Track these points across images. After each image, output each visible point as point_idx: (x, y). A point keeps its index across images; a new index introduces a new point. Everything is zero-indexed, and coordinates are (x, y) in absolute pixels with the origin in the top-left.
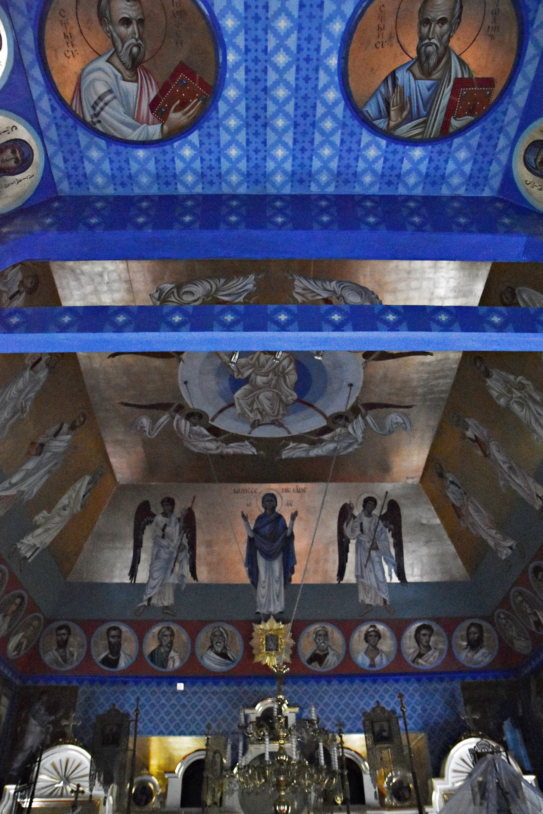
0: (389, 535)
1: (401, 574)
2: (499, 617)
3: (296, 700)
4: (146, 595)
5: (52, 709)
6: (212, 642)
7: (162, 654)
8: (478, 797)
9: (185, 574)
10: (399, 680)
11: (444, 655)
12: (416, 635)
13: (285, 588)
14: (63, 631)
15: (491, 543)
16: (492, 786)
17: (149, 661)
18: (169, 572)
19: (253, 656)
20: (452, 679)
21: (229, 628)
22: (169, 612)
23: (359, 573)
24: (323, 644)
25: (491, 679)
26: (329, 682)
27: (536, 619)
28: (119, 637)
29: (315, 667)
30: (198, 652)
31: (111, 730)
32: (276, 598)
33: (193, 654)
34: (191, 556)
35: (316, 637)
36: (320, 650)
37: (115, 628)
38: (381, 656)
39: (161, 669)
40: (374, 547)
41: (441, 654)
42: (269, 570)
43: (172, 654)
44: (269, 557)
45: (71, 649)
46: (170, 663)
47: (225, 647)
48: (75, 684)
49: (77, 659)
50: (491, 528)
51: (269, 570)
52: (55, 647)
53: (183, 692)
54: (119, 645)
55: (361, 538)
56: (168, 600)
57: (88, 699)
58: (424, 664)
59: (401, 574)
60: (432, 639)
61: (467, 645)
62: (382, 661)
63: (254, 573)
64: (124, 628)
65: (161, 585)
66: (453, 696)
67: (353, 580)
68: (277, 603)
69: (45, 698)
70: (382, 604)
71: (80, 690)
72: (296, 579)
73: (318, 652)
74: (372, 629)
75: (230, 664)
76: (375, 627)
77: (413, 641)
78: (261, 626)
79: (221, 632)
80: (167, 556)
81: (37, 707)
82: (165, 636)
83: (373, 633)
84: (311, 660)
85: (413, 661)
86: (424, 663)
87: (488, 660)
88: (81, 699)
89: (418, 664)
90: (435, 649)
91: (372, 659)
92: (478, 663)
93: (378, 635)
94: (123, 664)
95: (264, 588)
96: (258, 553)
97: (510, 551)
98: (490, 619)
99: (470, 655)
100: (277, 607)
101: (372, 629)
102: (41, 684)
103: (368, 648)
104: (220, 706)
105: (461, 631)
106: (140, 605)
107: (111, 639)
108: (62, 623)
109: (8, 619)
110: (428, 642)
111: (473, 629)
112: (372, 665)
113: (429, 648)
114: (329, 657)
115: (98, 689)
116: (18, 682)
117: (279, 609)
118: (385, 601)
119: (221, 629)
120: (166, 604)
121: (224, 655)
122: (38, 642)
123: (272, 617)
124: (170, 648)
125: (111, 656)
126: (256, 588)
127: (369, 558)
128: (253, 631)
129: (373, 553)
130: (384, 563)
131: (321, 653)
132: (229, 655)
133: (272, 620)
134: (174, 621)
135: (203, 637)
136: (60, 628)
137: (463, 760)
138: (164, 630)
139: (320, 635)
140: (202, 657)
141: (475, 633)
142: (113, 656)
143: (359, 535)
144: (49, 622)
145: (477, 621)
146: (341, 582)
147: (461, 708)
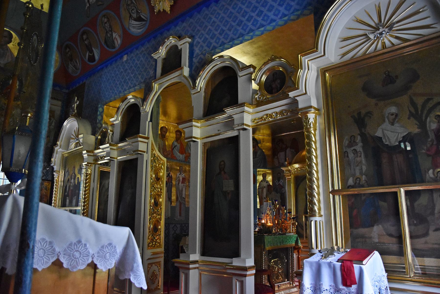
46: (115, 41)
94: (97, 57)
121: (139, 19)
132: (142, 16)
142: (91, 54)
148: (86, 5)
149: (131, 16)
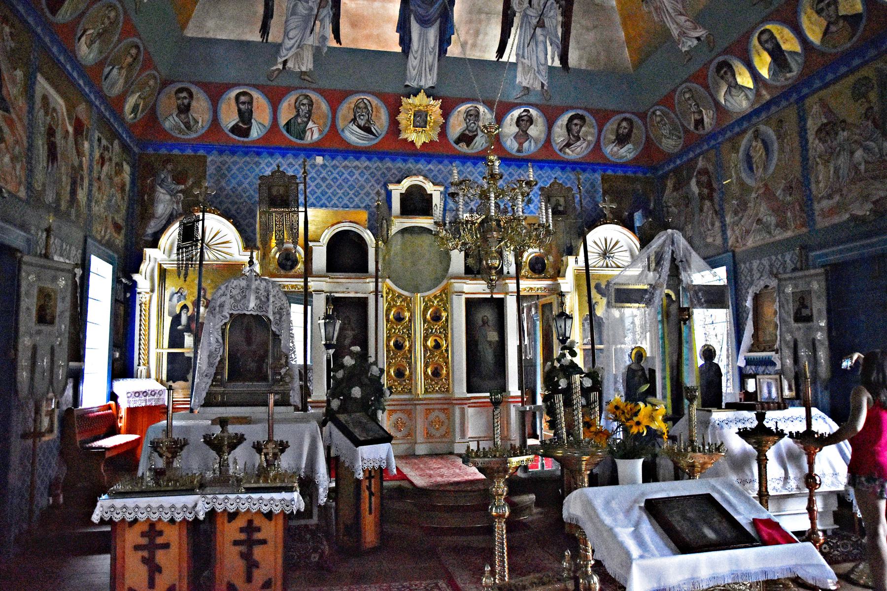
0: (559, 11)
1: (564, 58)
2: (654, 113)
3: (440, 179)
4: (281, 57)
5: (179, 179)
6: (355, 116)
7: (299, 124)
8: (653, 265)
9: (327, 35)
10: (544, 166)
11: (592, 146)
12: (567, 125)
13: (439, 60)
14: (184, 94)
15: (675, 33)
16: (667, 257)
17: (285, 133)
18: (308, 32)
19: (399, 131)
20: (594, 171)
21: (375, 101)
22: (307, 78)
23: (521, 53)
24: (473, 125)
25: (629, 174)
26: (475, 164)
27: (697, 117)
28: (250, 103)
29: (463, 148)
30: (340, 124)
31: (278, 191)
32: (428, 70)
33: (334, 125)
34: (334, 14)
35: (467, 116)
36: (470, 131)
37: (244, 94)
38: (530, 142)
39: (299, 141)
40: (541, 24)
41: (589, 145)
42: (423, 37)
43: (310, 125)
44: (425, 23)
45: (195, 115)
46: (308, 134)
47: (368, 120)
48: (201, 152)
49: (203, 127)
50: (681, 14)
51: (423, 37)
52: (175, 112)
53: (324, 166)
54: (251, 112)
55: (528, 12)
56: (307, 65)
57: (219, 169)
58: (571, 154)
59: (564, 58)
60: (583, 129)
61: (615, 140)
62: (530, 148)
63: (405, 41)
64: (256, 94)
65: (298, 47)
66: (593, 185)
67: (513, 59)
68: (429, 77)
69: (169, 167)
70: (539, 88)
71: (209, 159)
72: (453, 51)
73: (467, 132)
74: (525, 114)
75: (372, 139)
76: (528, 111)
77: (564, 131)
78: (410, 101)
79: (365, 104)
80: (306, 12)
81: (163, 176)
82: (303, 105)
83: (525, 118)
84: (458, 141)
85: (561, 150)
86: (570, 153)
87: (630, 156)
88: (211, 170)
89: (565, 153)
90: (584, 140)
91: (521, 144)
92: (622, 157)
93: (531, 121)
95: (415, 58)
96: (412, 18)
97: (696, 42)
98: (643, 116)
99: (615, 149)
100: (429, 80)
101: (525, 114)
102: (164, 151)
103: (518, 133)
104: (362, 180)
105: (611, 126)
106: (275, 68)
107: (242, 107)
108: (180, 85)
109: (124, 72)
110: (579, 132)
111: (624, 124)
112: (519, 151)
113: (578, 138)
114: (477, 138)
115: (228, 159)
116: (136, 150)
117: (430, 84)
118: (543, 85)
119: (365, 101)
120: (304, 69)
121: (367, 130)
122: (155, 105)
123: (422, 91)
124: (309, 119)
125: (240, 124)
126: (408, 57)
127: (533, 36)
128: (402, 105)
129: (539, 31)
130: (548, 43)
131: (470, 135)
132: (373, 129)
133: (422, 95)
134: (314, 90)
135: (345, 109)
136: (181, 90)
137: (606, 240)
138: (301, 98)
139: (471, 115)
140: (343, 130)
141: (625, 128)
142: (245, 124)
143: (527, 8)
144: (165, 84)
145: (628, 115)
146: (500, 60)
147: (599, 198)
148: (276, 63)
149: (354, 120)
